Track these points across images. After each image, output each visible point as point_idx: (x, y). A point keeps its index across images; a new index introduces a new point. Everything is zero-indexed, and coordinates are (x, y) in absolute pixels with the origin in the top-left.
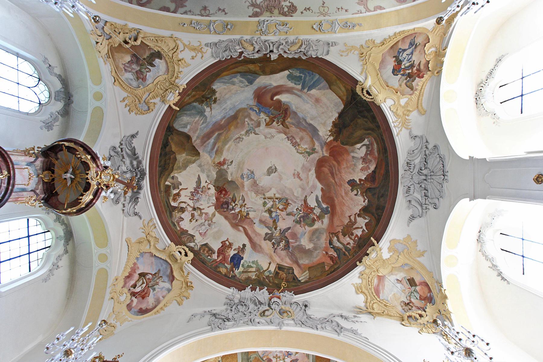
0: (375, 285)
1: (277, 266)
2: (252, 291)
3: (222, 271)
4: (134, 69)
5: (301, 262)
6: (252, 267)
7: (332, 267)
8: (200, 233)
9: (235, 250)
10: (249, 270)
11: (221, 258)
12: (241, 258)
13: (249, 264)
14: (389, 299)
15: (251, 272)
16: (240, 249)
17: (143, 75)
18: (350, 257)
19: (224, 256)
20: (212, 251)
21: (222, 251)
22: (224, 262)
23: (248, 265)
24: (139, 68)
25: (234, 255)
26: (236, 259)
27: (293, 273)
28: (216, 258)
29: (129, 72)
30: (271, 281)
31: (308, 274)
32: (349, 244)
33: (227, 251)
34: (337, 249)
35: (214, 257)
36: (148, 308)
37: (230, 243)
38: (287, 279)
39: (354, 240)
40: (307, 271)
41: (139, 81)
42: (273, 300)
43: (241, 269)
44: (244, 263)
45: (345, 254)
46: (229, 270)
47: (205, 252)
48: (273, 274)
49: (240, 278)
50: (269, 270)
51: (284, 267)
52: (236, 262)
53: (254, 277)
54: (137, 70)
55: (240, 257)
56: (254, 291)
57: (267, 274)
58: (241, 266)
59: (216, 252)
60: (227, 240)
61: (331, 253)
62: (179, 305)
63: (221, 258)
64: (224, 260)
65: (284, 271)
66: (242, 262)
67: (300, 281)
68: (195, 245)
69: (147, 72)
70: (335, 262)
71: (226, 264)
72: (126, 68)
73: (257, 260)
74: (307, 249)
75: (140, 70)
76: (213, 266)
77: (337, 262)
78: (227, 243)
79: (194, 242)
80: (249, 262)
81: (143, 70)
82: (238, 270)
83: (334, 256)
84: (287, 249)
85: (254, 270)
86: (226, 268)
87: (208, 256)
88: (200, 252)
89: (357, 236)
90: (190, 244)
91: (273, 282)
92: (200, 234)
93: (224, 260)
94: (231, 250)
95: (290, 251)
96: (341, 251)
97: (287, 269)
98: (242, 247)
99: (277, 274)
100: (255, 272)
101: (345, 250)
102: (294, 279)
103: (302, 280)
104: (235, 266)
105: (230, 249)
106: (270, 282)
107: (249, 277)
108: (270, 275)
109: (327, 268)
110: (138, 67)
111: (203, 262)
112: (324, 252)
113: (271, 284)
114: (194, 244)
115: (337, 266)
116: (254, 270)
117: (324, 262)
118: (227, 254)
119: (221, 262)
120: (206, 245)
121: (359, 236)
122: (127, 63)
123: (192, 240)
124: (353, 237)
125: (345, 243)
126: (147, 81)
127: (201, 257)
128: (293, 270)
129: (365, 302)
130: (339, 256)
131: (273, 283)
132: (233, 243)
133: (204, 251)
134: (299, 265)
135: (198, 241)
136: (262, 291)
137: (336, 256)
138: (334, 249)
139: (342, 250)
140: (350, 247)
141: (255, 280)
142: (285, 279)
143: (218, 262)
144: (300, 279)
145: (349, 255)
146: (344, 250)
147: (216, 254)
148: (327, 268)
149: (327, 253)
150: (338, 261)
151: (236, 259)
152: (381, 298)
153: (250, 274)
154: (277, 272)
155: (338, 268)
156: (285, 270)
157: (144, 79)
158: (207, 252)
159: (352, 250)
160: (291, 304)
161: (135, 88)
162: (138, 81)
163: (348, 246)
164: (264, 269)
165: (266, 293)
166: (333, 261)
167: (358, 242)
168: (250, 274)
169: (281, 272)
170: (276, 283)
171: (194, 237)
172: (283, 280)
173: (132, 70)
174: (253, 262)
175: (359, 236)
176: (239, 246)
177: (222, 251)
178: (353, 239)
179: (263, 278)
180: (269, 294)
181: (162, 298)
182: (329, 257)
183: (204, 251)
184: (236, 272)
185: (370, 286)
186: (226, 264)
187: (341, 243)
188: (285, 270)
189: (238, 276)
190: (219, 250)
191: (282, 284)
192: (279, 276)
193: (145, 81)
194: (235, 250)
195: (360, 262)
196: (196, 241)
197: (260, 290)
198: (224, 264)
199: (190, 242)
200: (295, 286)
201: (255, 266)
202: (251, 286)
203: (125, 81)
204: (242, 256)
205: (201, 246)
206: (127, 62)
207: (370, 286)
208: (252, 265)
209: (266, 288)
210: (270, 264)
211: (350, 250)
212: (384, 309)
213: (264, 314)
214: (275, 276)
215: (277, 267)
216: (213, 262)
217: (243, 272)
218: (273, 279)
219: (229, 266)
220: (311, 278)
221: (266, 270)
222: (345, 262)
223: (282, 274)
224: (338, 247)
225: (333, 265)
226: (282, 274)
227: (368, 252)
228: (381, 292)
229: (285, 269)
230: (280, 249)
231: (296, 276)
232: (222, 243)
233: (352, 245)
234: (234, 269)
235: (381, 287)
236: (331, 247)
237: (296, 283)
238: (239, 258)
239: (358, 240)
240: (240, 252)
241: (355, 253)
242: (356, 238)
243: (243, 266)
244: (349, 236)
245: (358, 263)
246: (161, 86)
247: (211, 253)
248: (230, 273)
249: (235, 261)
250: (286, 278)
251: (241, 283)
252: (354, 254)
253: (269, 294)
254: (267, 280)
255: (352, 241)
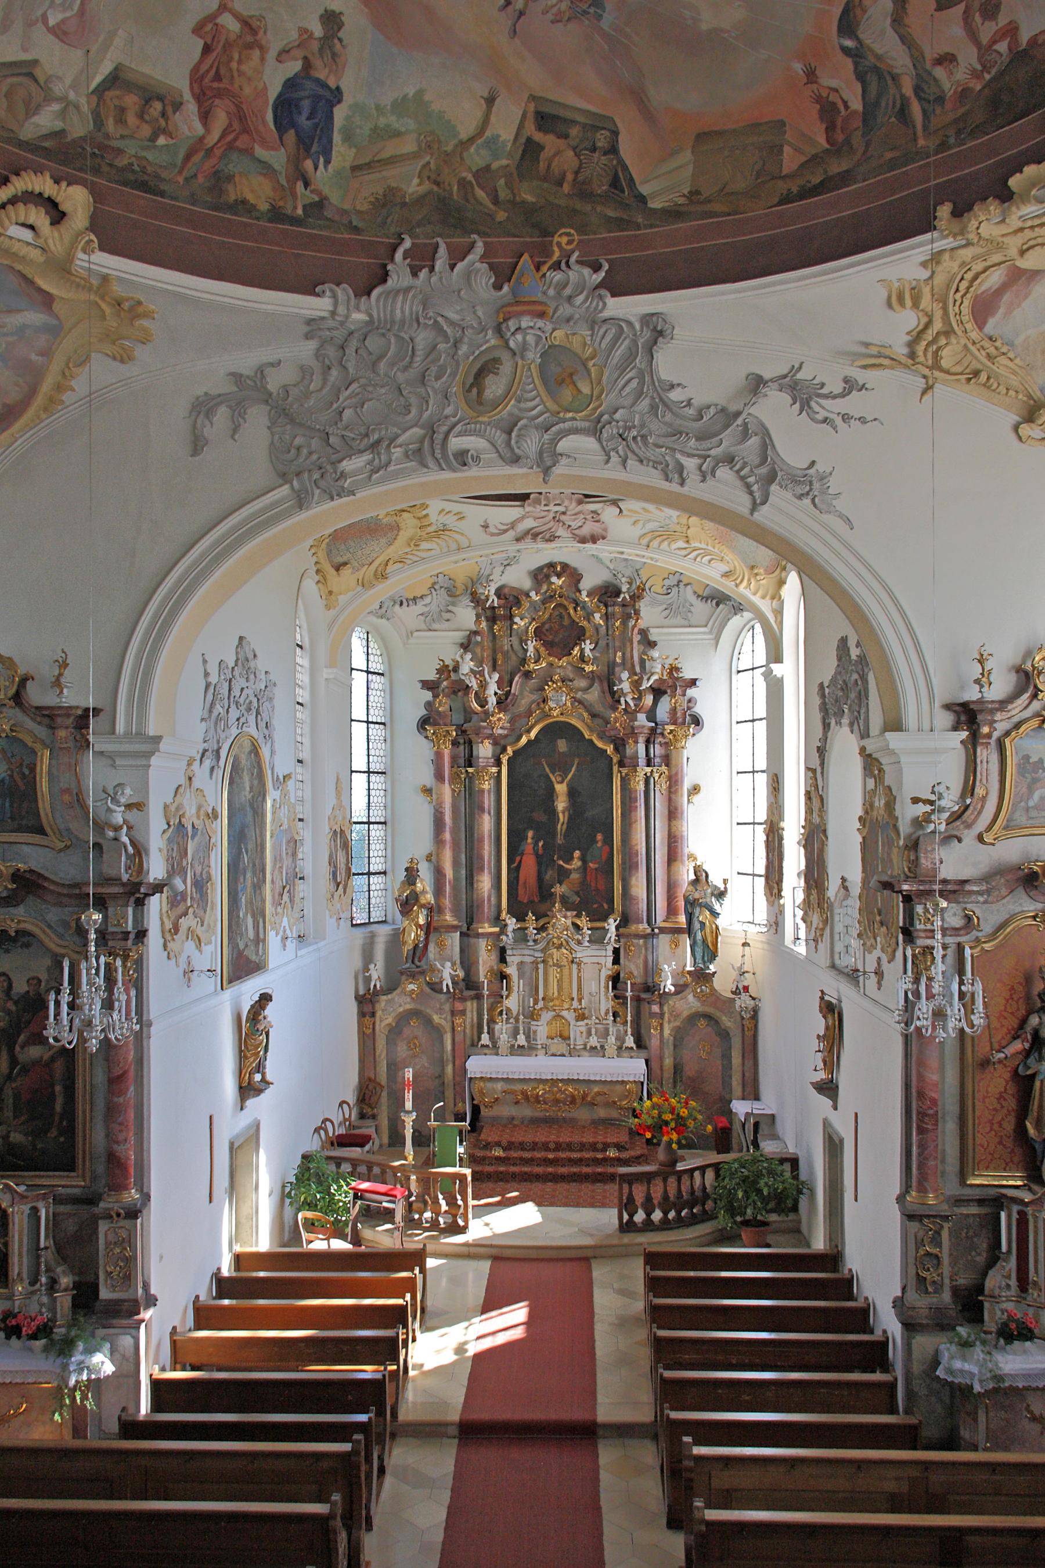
0: (983, 288)
1: (532, 107)
2: (415, 274)
3: (251, 198)
5: (658, 96)
6: (398, 134)
7: (815, 160)
8: (52, 31)
9: (283, 54)
10: (385, 155)
11: (220, 120)
12: (328, 94)
13: (382, 121)
14: (1019, 341)
15: (392, 161)
16: (315, 46)
18: (921, 142)
19: (239, 107)
20: (160, 98)
21: (218, 77)
22: (245, 137)
23: (375, 130)
25: (290, 84)
26: (306, 104)
27: (613, 150)
28: (200, 130)
30: (503, 194)
31: (691, 167)
32: (947, 59)
33: (241, 74)
34: (876, 69)
35: (185, 130)
36: (8, 402)
37: (245, 23)
38: (581, 177)
39: (984, 51)
40: (687, 156)
42: (512, 324)
43: (342, 154)
44: (348, 118)
45: (903, 113)
46: (283, 181)
47: (132, 119)
48: (510, 155)
49: (346, 207)
50: (488, 133)
51: (562, 113)
52: (309, 123)
53: (414, 187)
55: (321, 91)
56: (424, 273)
57: (477, 157)
58: (337, 138)
59: (187, 96)
60: (223, 8)
61: (833, 83)
62: (122, 361)
63: (220, 120)
64: (246, 131)
65: (566, 136)
66: (340, 113)
67: (642, 199)
68: (63, 114)
70: (840, 137)
71: (260, 152)
73: (420, 93)
74: (704, 27)
76: (201, 179)
77: (847, 142)
78: (230, 24)
79: (49, 98)
80: (378, 108)
82: (327, 162)
83: (846, 104)
84: (585, 13)
85: (409, 146)
86: (267, 169)
87: (153, 138)
88: (107, 136)
89: (1011, 31)
90: (35, 119)
91: (513, 203)
92: (59, 32)
93: (246, 131)
94: (263, 59)
95: (605, 24)
96: (892, 90)
97: (584, 126)
98: (318, 31)
99: (531, 150)
100: (415, 156)
101: (918, 89)
102: (615, 183)
103: (654, 195)
104: (307, 150)
105: (257, 53)
106: (496, 201)
107: (391, 191)
108: (495, 165)
109: (790, 161)
111: (144, 186)
112: (798, 67)
113: (501, 216)
114: (56, 107)
115: (844, 166)
116: (409, 146)
117: (782, 124)
118: (247, 91)
119: (230, 147)
120: (115, 79)
121: (1025, 37)
123: (33, 88)
124: (987, 30)
125: (930, 54)
127: (121, 162)
128: (615, 133)
129: (914, 333)
130: (870, 108)
131: (514, 204)
132: (260, 19)
133: (121, 121)
134: (647, 114)
135: (68, 81)
136: (460, 266)
137: (857, 105)
138: (856, 64)
139: (899, 87)
140: (946, 85)
141: (420, 200)
142: (570, 177)
143: (218, 152)
144: (644, 190)
145: (925, 128)
146: (908, 90)
147: (191, 107)
148: (790, 161)
149: (811, 75)
150: (857, 140)
151: (306, 104)
152: (990, 327)
153: (392, 176)
154: (529, 140)
155: (845, 178)
156: (574, 131)
158: (141, 116)
159: (948, 105)
160: (594, 322)
163: (939, 72)
164: (464, 136)
165: (484, 279)
166: (830, 129)
167: (1001, 74)
168: (392, 176)
169: (548, 141)
170: (523, 202)
171: (38, 72)
172: (560, 183)
174: (400, 106)
175: (1025, 37)
176: (303, 31)
177: (218, 77)
178: (985, 40)
179: (463, 183)
180: (498, 287)
181: (40, 358)
182: (819, 99)
183: (121, 121)
184: (323, 176)
185: (958, 296)
186: (260, 152)
187: (906, 40)
188: (574, 131)
189: (335, 198)
190: (196, 77)
191: (556, 239)
192: (542, 165)
194: (283, 54)
195: (957, 213)
196: (58, 89)
197: (458, 255)
198: (248, 152)
199: (32, 109)
200: (621, 224)
201: (411, 124)
202: (407, 244)
204: (332, 83)
205: (95, 99)
207: (958, 296)
208: (396, 125)
209: (479, 248)
210: (490, 101)
211: (940, 99)
212: (980, 367)
213: (480, 393)
214: (518, 168)
215: (531, 117)
216: (188, 158)
217: (355, 168)
218: (509, 185)
219: (278, 158)
220: (698, 193)
221: (472, 140)
222: (889, 155)
223: (558, 153)
224: (878, 57)
225: (826, 151)
226: (558, 153)
227: (1014, 182)
228: (1001, 311)
229: (574, 122)
230: (545, 12)
231: (625, 168)
232: (198, 30)
233: (961, 74)
234: (308, 164)
235: (1007, 297)
236: (846, 51)
237: (626, 207)
238: (316, 98)
239: (1005, 59)
240: (317, 63)
241: (959, 132)
242: (1002, 47)
243: (348, 137)
244: (967, 15)
245: (944, 211)
247: (164, 114)
248: (294, 194)
249: (303, 120)
250: (577, 173)
251: (356, 230)
252: (951, 132)
253: (498, 287)
254: (480, 194)
255: (974, 51)
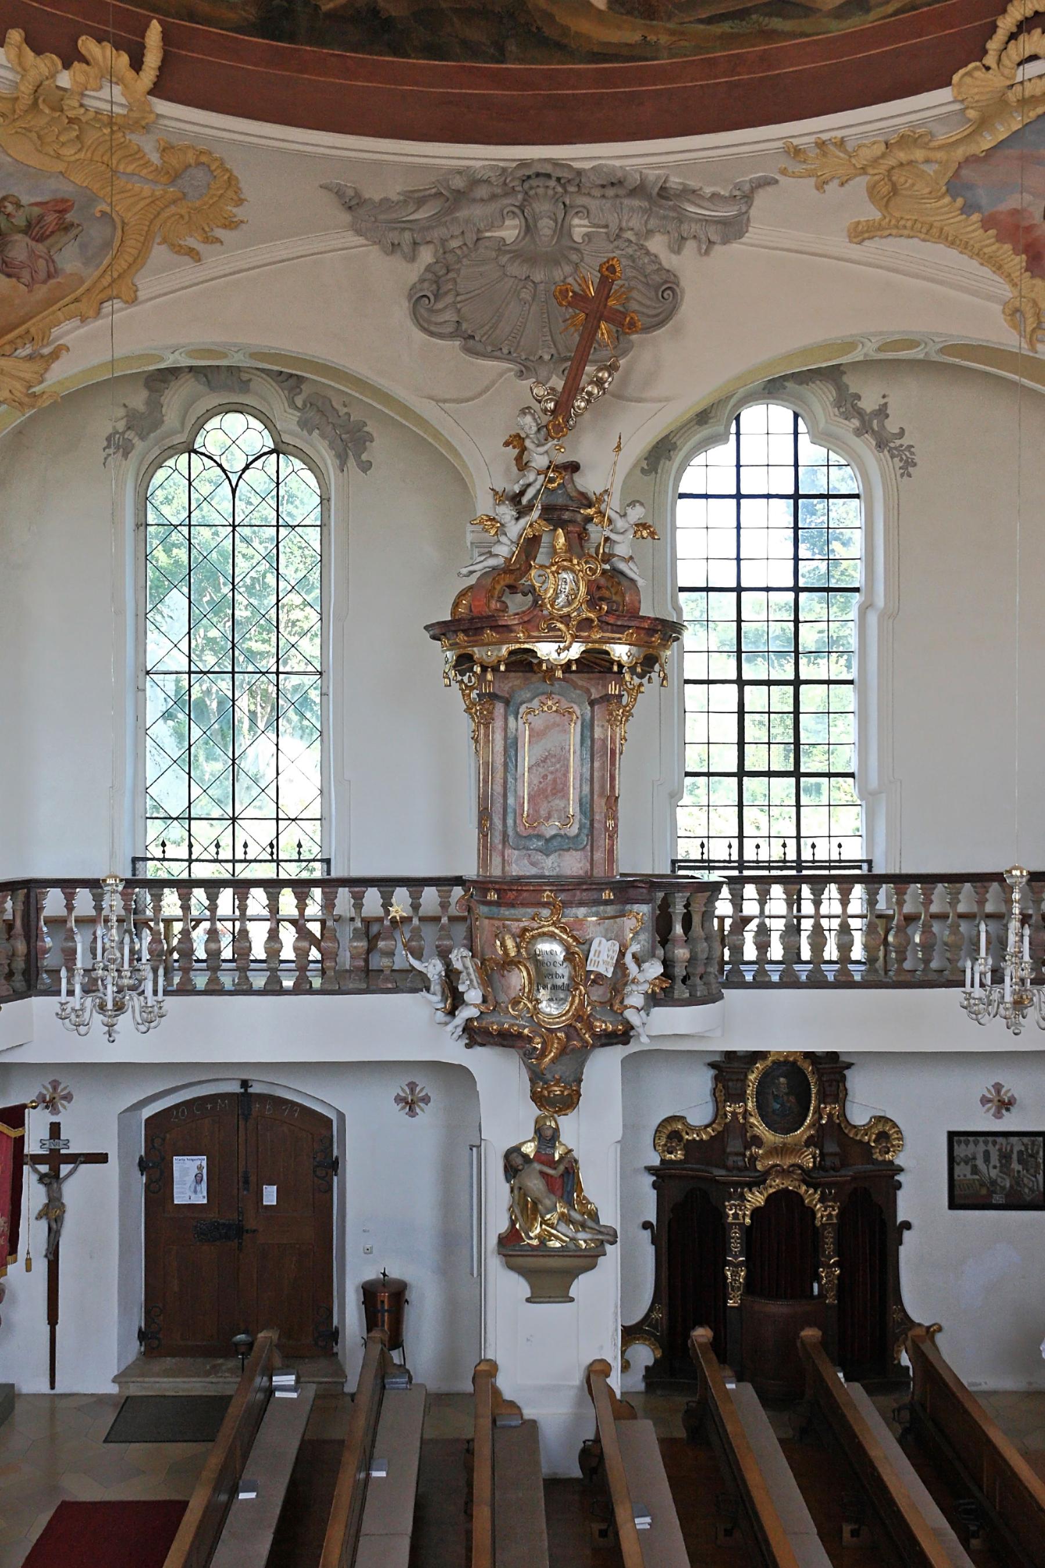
4: (32, 253)
17: (41, 218)
24: (18, 236)
29: (53, 262)
41: (76, 222)
54: (27, 239)
69: (18, 205)
72: (42, 275)
75: (27, 230)
81: (20, 221)
110: (16, 241)
122: (18, 278)
126: (59, 196)
157: (61, 207)
161: (115, 228)
162: (78, 225)
173: (41, 257)
193: (64, 201)
203: (98, 266)
206: (14, 280)
246: (62, 139)
